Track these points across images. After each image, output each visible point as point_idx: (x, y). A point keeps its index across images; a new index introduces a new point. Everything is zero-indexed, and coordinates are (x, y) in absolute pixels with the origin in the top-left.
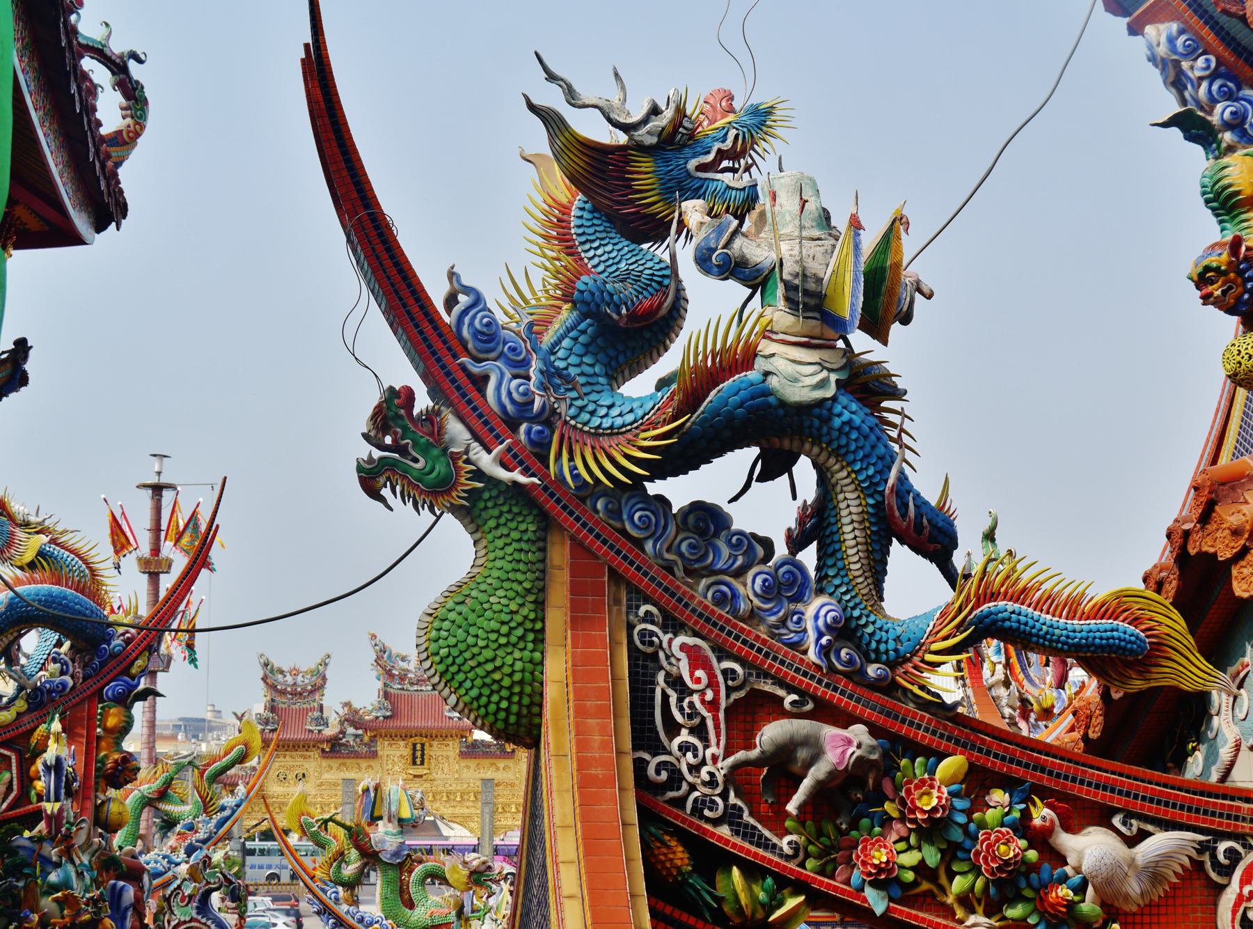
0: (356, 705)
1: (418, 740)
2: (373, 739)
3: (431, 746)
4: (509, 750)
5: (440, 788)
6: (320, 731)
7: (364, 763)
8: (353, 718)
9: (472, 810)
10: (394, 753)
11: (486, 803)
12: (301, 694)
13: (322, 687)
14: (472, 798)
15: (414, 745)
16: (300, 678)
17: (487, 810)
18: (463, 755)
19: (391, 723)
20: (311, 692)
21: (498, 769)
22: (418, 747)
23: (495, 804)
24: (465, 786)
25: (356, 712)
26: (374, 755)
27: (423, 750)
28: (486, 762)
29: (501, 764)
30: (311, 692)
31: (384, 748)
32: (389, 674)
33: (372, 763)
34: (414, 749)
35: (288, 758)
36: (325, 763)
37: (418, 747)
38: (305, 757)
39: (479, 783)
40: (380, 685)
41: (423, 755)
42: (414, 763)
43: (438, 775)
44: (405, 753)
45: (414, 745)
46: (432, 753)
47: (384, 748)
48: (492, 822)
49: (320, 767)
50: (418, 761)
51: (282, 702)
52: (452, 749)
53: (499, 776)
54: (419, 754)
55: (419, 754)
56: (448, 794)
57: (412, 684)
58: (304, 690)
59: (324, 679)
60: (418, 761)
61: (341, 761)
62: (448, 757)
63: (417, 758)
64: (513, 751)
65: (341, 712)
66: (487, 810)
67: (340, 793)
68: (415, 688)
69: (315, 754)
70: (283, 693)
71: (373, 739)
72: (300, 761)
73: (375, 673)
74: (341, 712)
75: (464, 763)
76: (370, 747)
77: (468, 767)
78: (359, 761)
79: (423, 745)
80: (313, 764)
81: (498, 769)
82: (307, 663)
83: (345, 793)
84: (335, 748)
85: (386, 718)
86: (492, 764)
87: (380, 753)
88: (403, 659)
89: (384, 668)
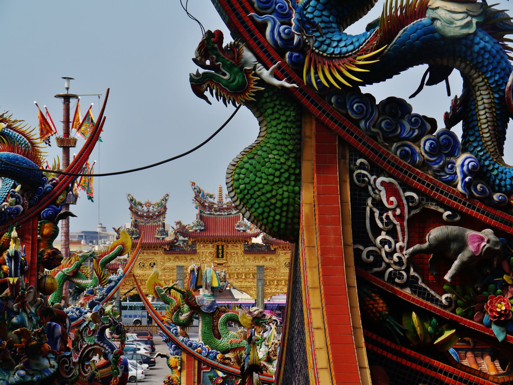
0: (184, 223)
1: (220, 243)
2: (194, 243)
3: (227, 247)
4: (272, 249)
5: (233, 271)
6: (163, 238)
7: (189, 257)
8: (182, 230)
9: (252, 284)
10: (206, 251)
11: (259, 280)
12: (152, 217)
13: (164, 213)
14: (252, 277)
15: (218, 246)
16: (151, 208)
18: (246, 252)
19: (204, 234)
20: (158, 216)
21: (266, 260)
22: (220, 247)
23: (265, 280)
24: (247, 270)
25: (184, 227)
26: (194, 252)
27: (223, 249)
28: (260, 256)
29: (268, 257)
30: (158, 216)
31: (200, 248)
32: (203, 205)
33: (194, 257)
34: (218, 249)
35: (145, 254)
36: (166, 257)
37: (220, 247)
38: (155, 253)
39: (255, 268)
40: (197, 211)
41: (223, 252)
42: (218, 257)
43: (232, 264)
44: (213, 251)
45: (218, 246)
46: (228, 251)
47: (200, 248)
48: (263, 290)
49: (164, 259)
50: (220, 256)
51: (141, 222)
52: (240, 249)
53: (267, 264)
54: (220, 251)
55: (220, 251)
56: (238, 274)
57: (216, 211)
58: (154, 215)
59: (165, 208)
60: (220, 256)
61: (175, 256)
62: (237, 253)
63: (219, 254)
64: (275, 249)
65: (175, 227)
66: (260, 283)
68: (218, 213)
69: (160, 252)
70: (142, 216)
71: (194, 243)
72: (152, 256)
73: (195, 205)
74: (175, 227)
75: (246, 257)
76: (192, 247)
77: (249, 259)
78: (186, 255)
79: (223, 246)
80: (159, 257)
81: (266, 260)
82: (156, 199)
83: (178, 274)
84: (172, 248)
85: (201, 230)
86: (263, 257)
87: (198, 251)
88: (211, 196)
89: (200, 202)
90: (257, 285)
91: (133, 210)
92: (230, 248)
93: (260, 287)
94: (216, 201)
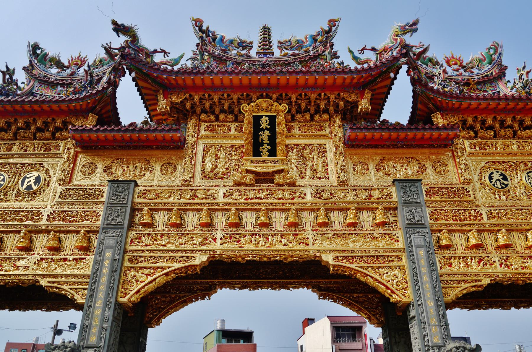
15: (257, 120)
17: (417, 240)
18: (352, 144)
22: (264, 123)
24: (363, 195)
26: (178, 146)
36: (83, 160)
37: (264, 123)
45: (257, 120)
54: (265, 136)
55: (265, 136)
67: (101, 210)
83: (110, 206)
90: (410, 245)
91: (35, 72)
92: (296, 132)
93: (422, 253)
94: (253, 53)
